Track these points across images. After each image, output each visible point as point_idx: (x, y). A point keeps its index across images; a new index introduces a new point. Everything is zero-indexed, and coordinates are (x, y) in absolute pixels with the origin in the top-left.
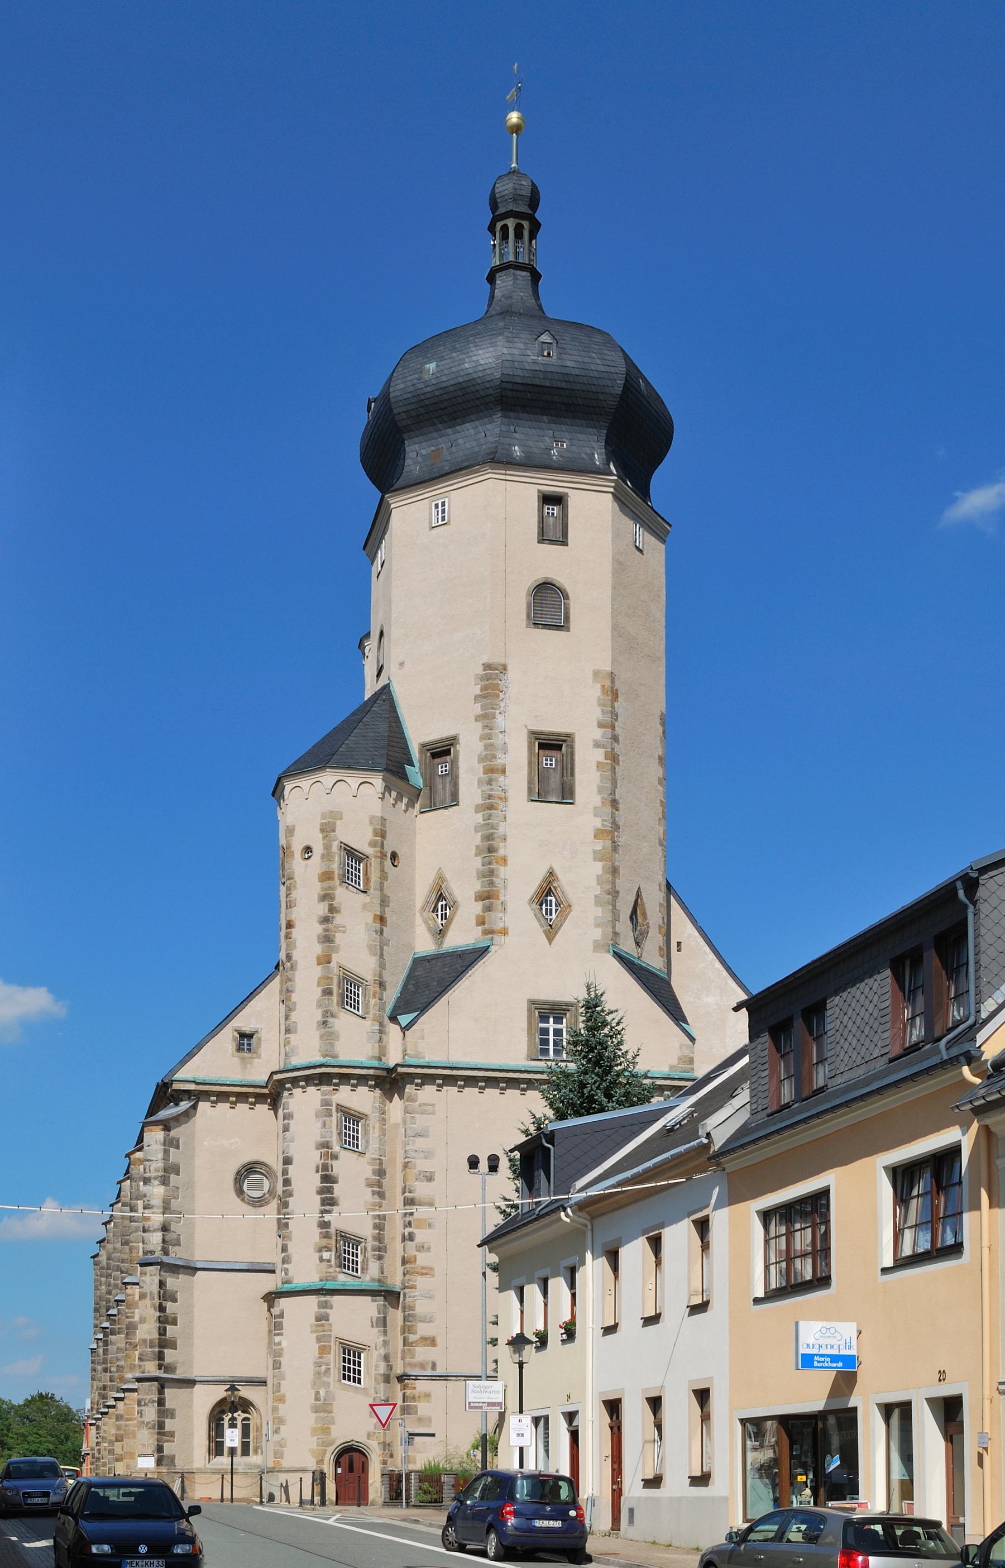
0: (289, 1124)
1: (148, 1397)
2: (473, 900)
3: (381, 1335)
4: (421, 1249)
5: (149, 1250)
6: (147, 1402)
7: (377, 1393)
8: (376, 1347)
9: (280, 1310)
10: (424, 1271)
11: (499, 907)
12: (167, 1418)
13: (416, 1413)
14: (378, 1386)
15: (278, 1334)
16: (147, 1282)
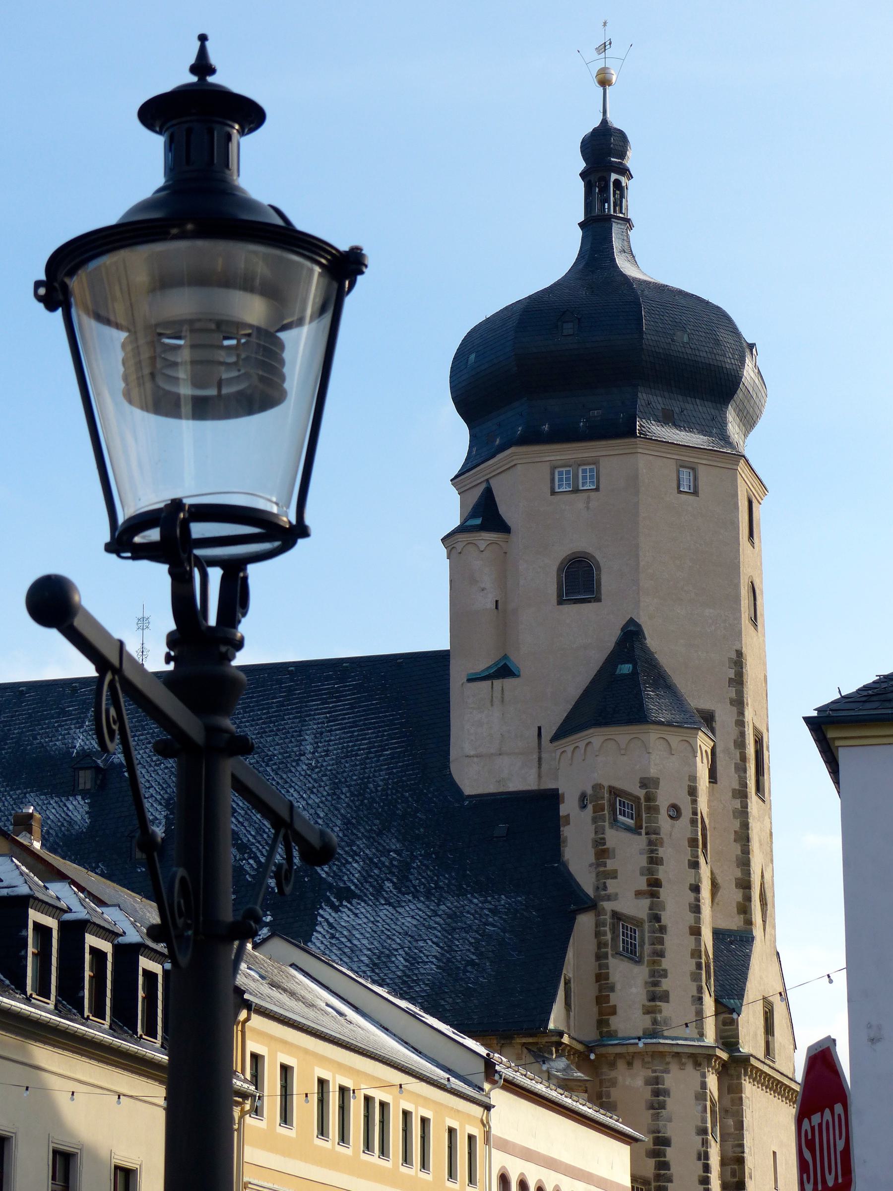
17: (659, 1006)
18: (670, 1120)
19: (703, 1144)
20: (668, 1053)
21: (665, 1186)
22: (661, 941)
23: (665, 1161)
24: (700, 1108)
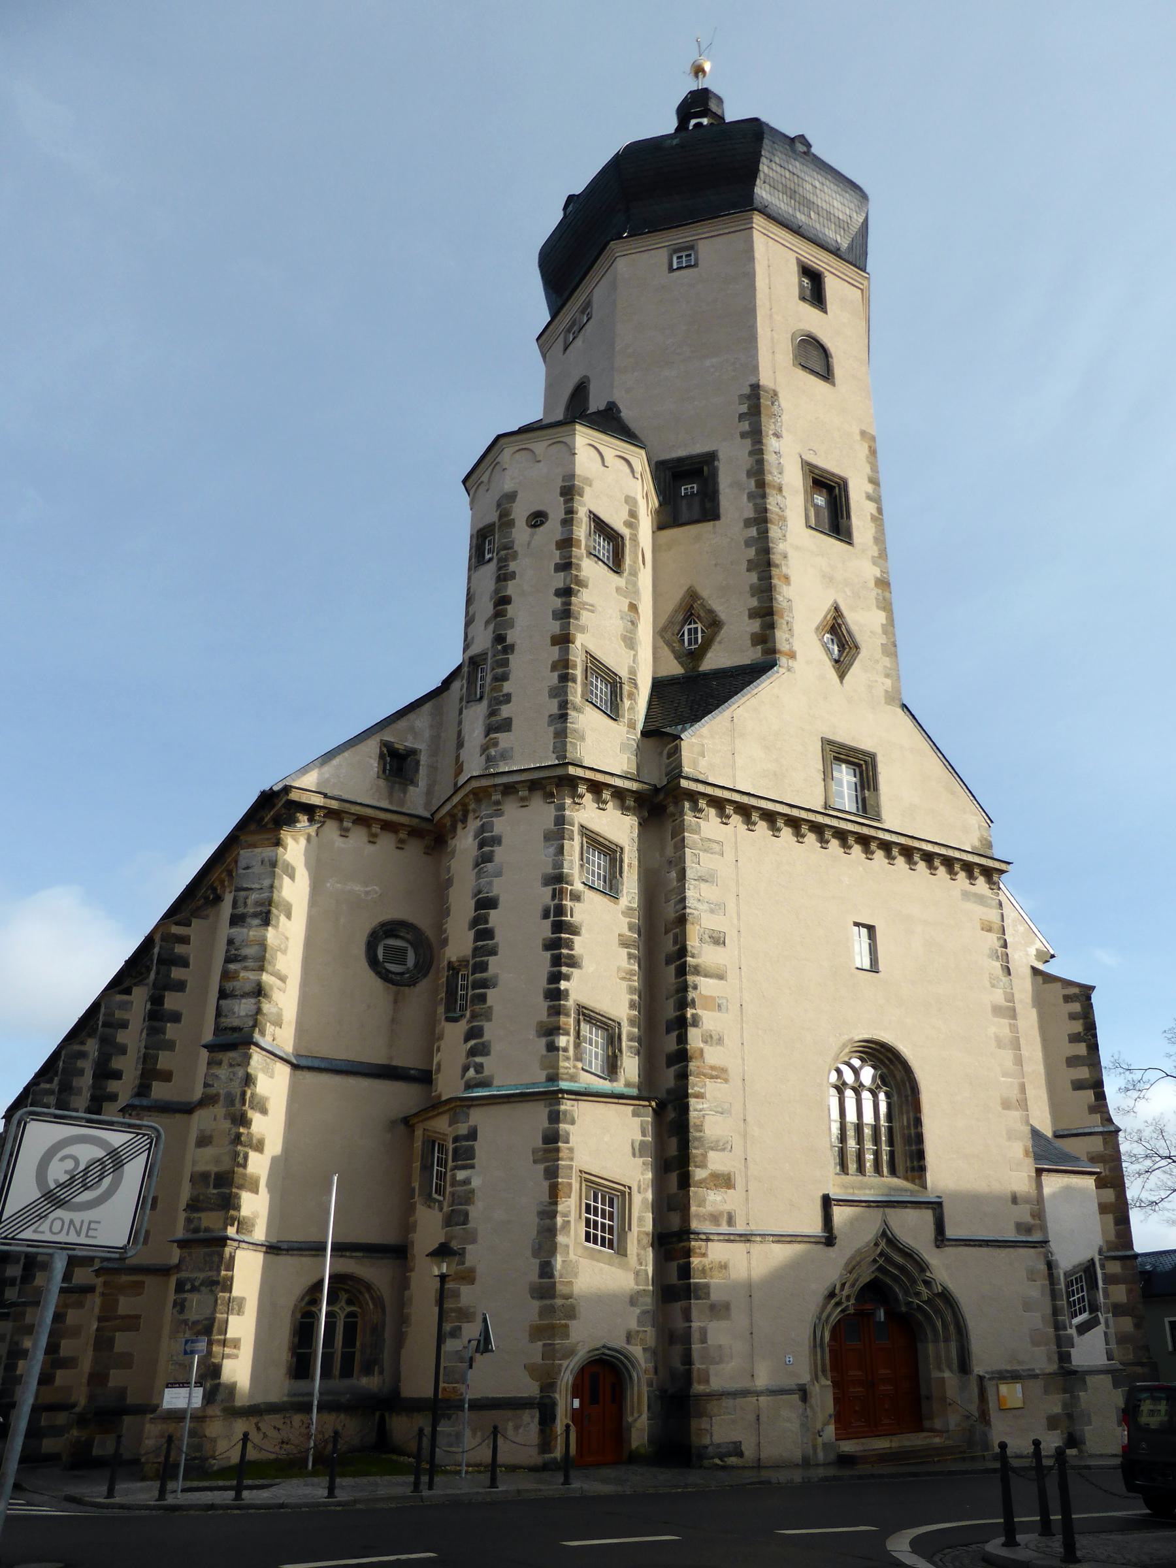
0: (492, 852)
1: (201, 1276)
2: (746, 618)
3: (647, 1169)
4: (709, 1040)
5: (230, 1026)
6: (197, 1284)
7: (641, 1264)
8: (639, 1187)
9: (470, 1127)
10: (714, 1073)
11: (784, 626)
12: (232, 1314)
13: (707, 1295)
14: (642, 1252)
15: (464, 1167)
16: (223, 1077)
17: (496, 738)
18: (499, 874)
19: (554, 897)
20: (493, 789)
21: (483, 961)
22: (505, 663)
23: (487, 928)
24: (552, 850)
